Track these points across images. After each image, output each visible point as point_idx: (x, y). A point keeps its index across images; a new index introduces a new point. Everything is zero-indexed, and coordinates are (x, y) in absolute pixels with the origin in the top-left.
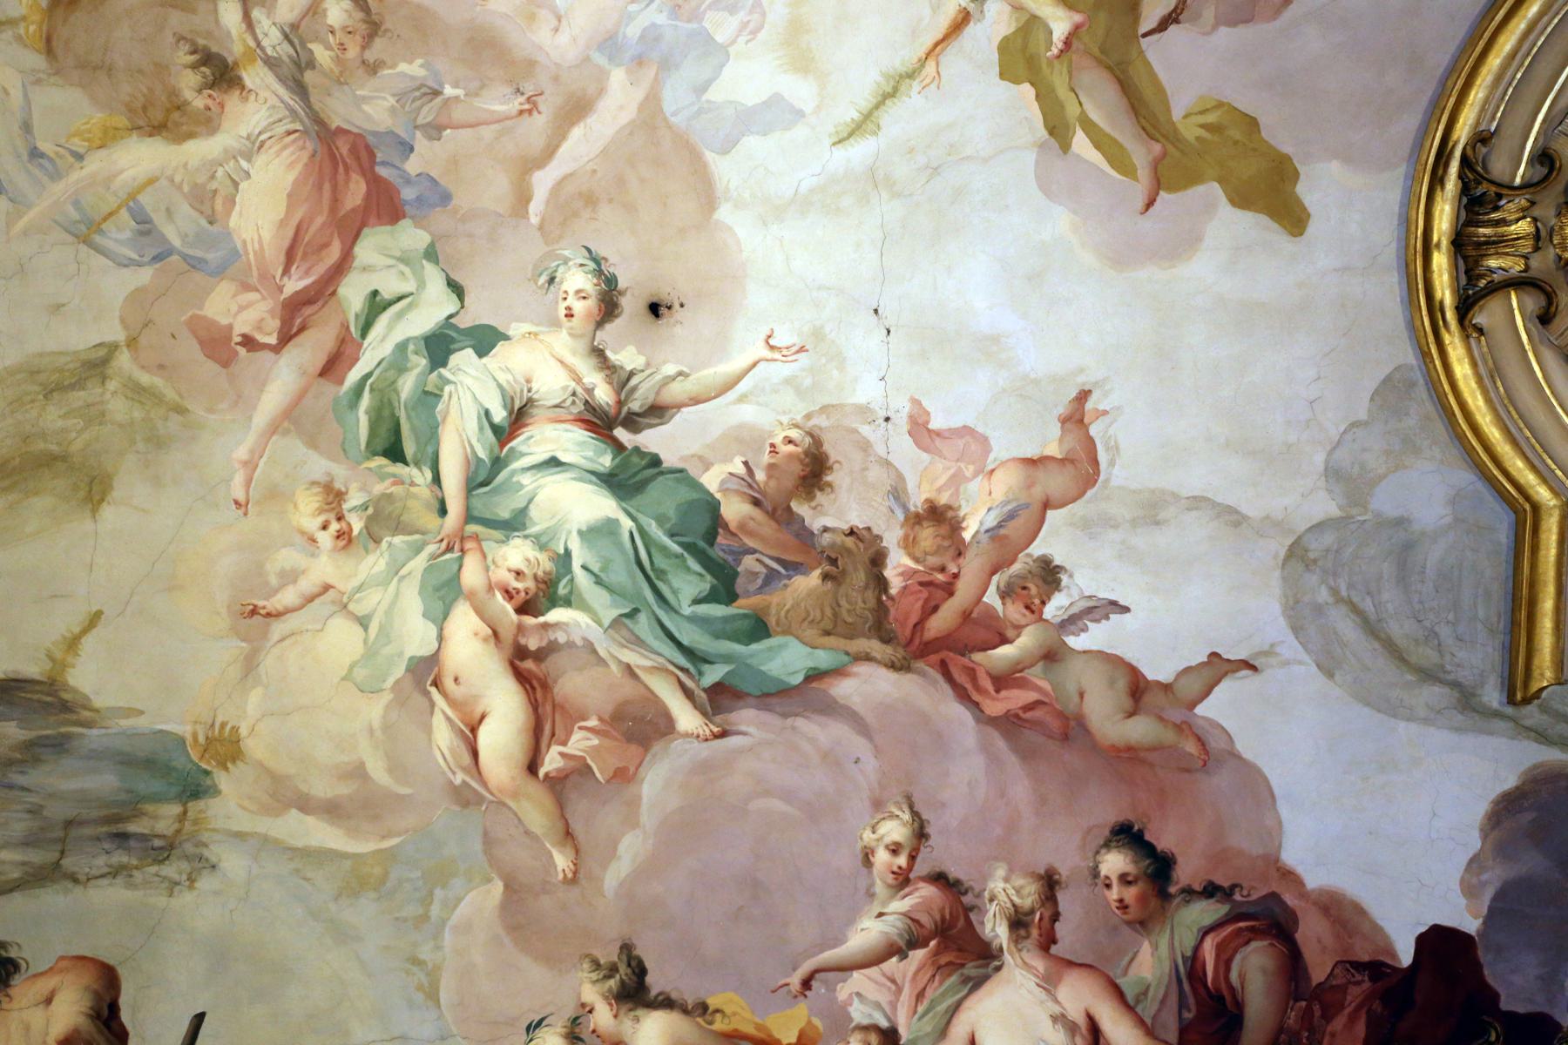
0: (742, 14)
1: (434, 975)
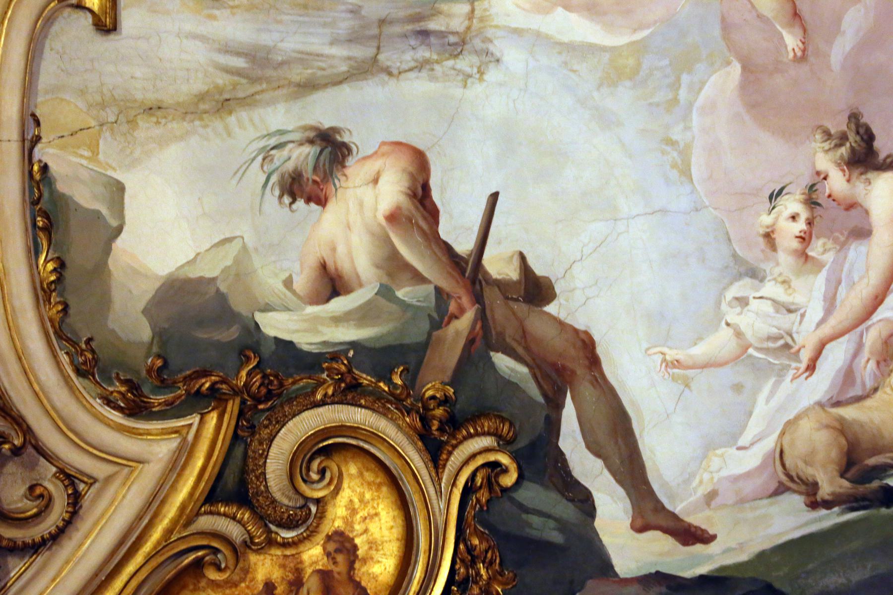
1: (685, 153)
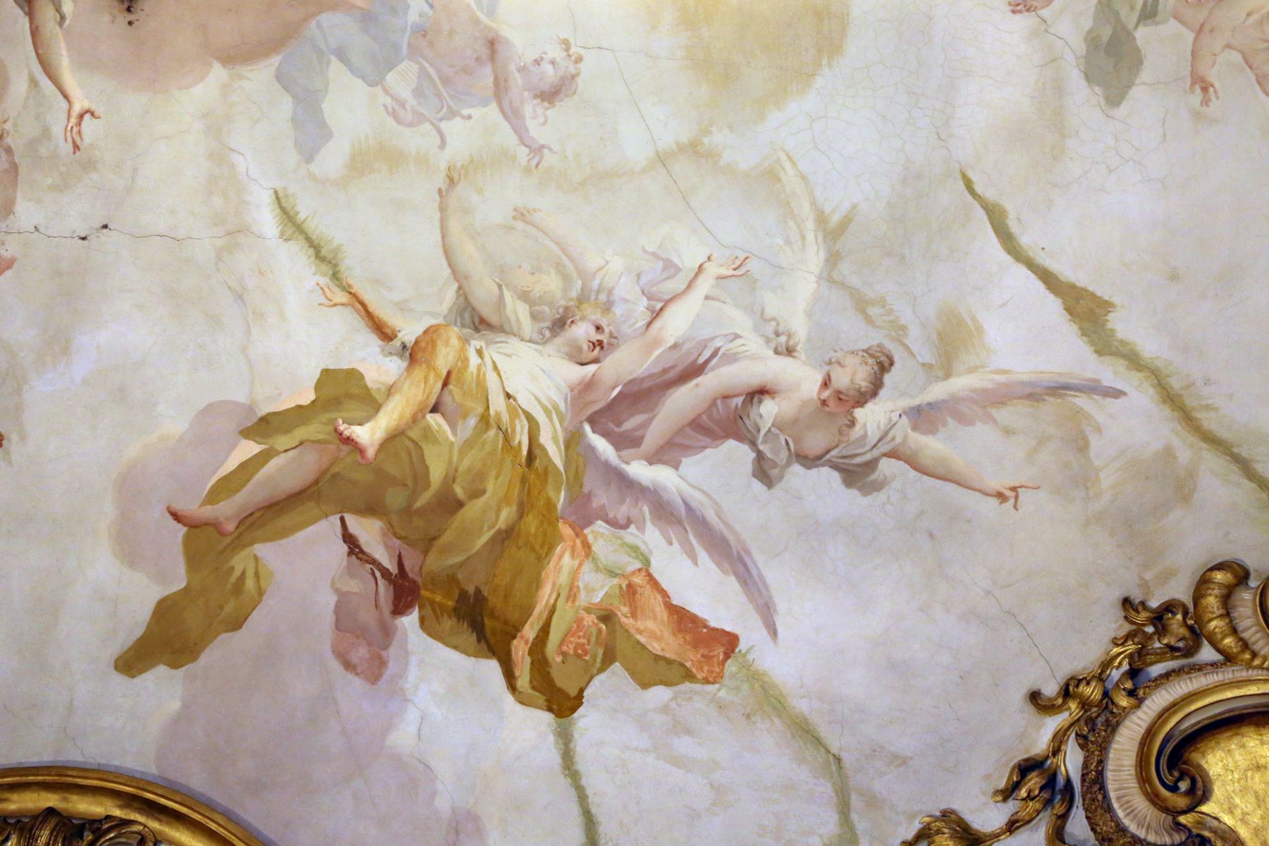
0: (414, 103)
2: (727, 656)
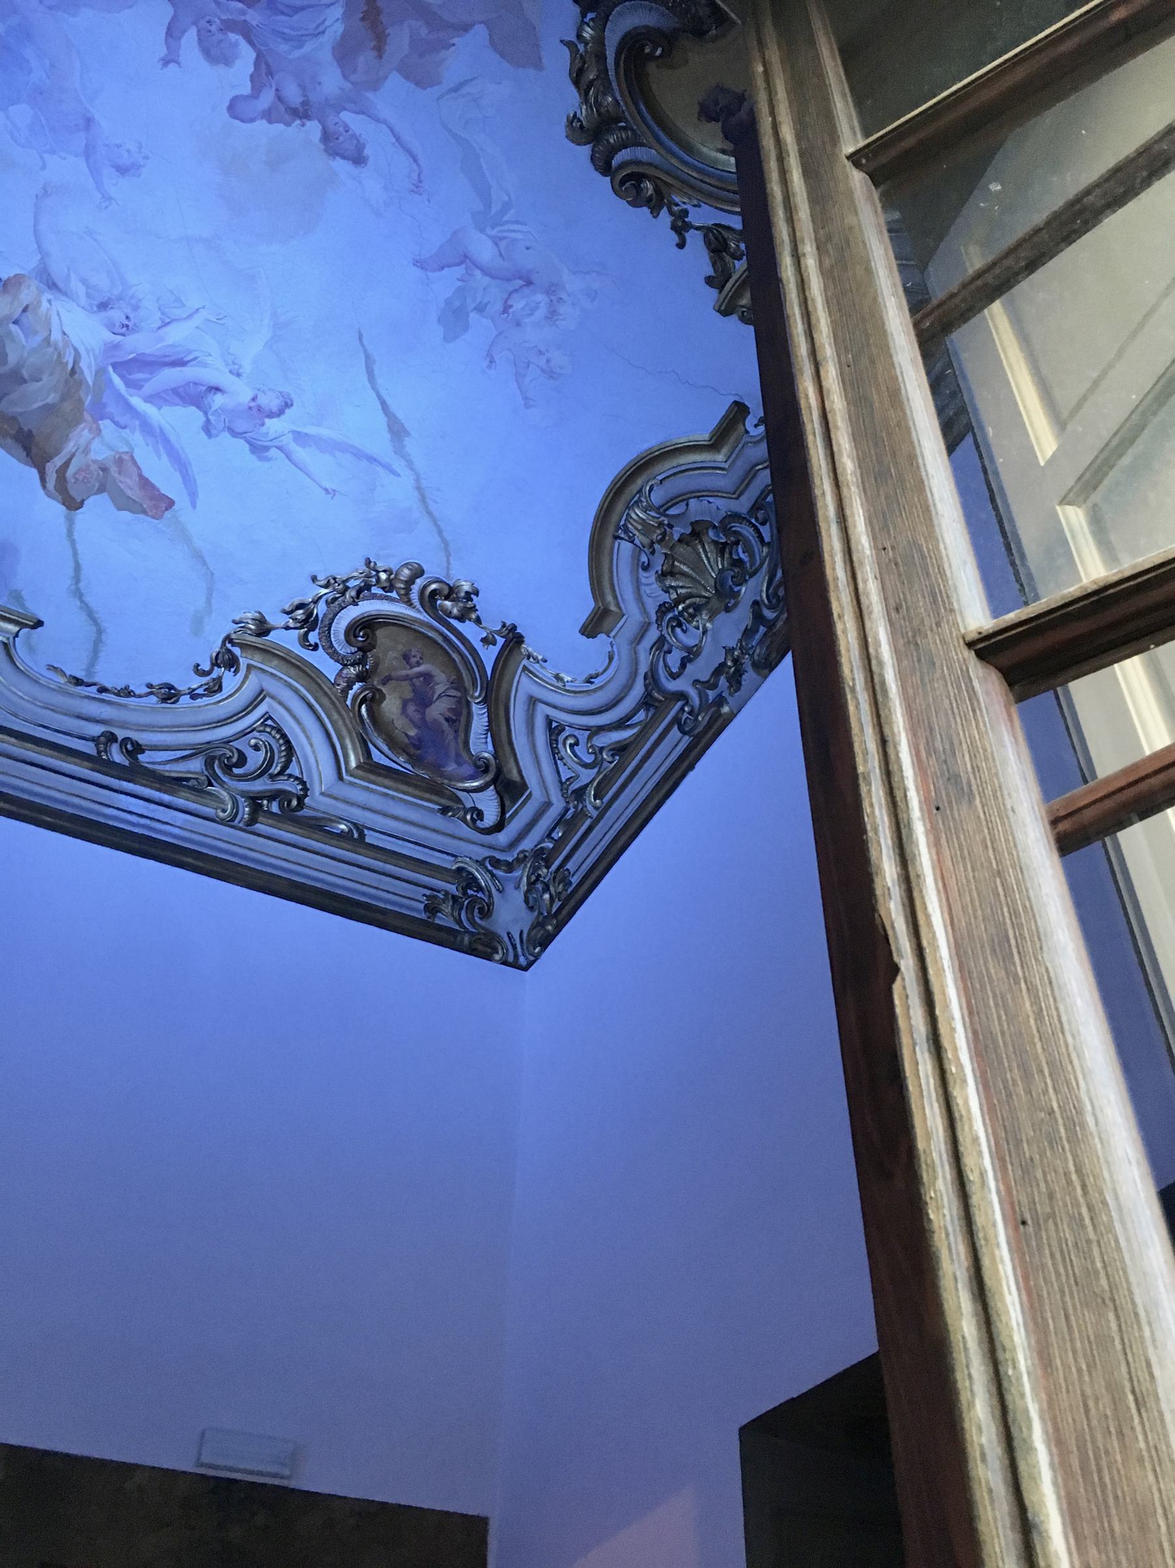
2: (167, 509)
